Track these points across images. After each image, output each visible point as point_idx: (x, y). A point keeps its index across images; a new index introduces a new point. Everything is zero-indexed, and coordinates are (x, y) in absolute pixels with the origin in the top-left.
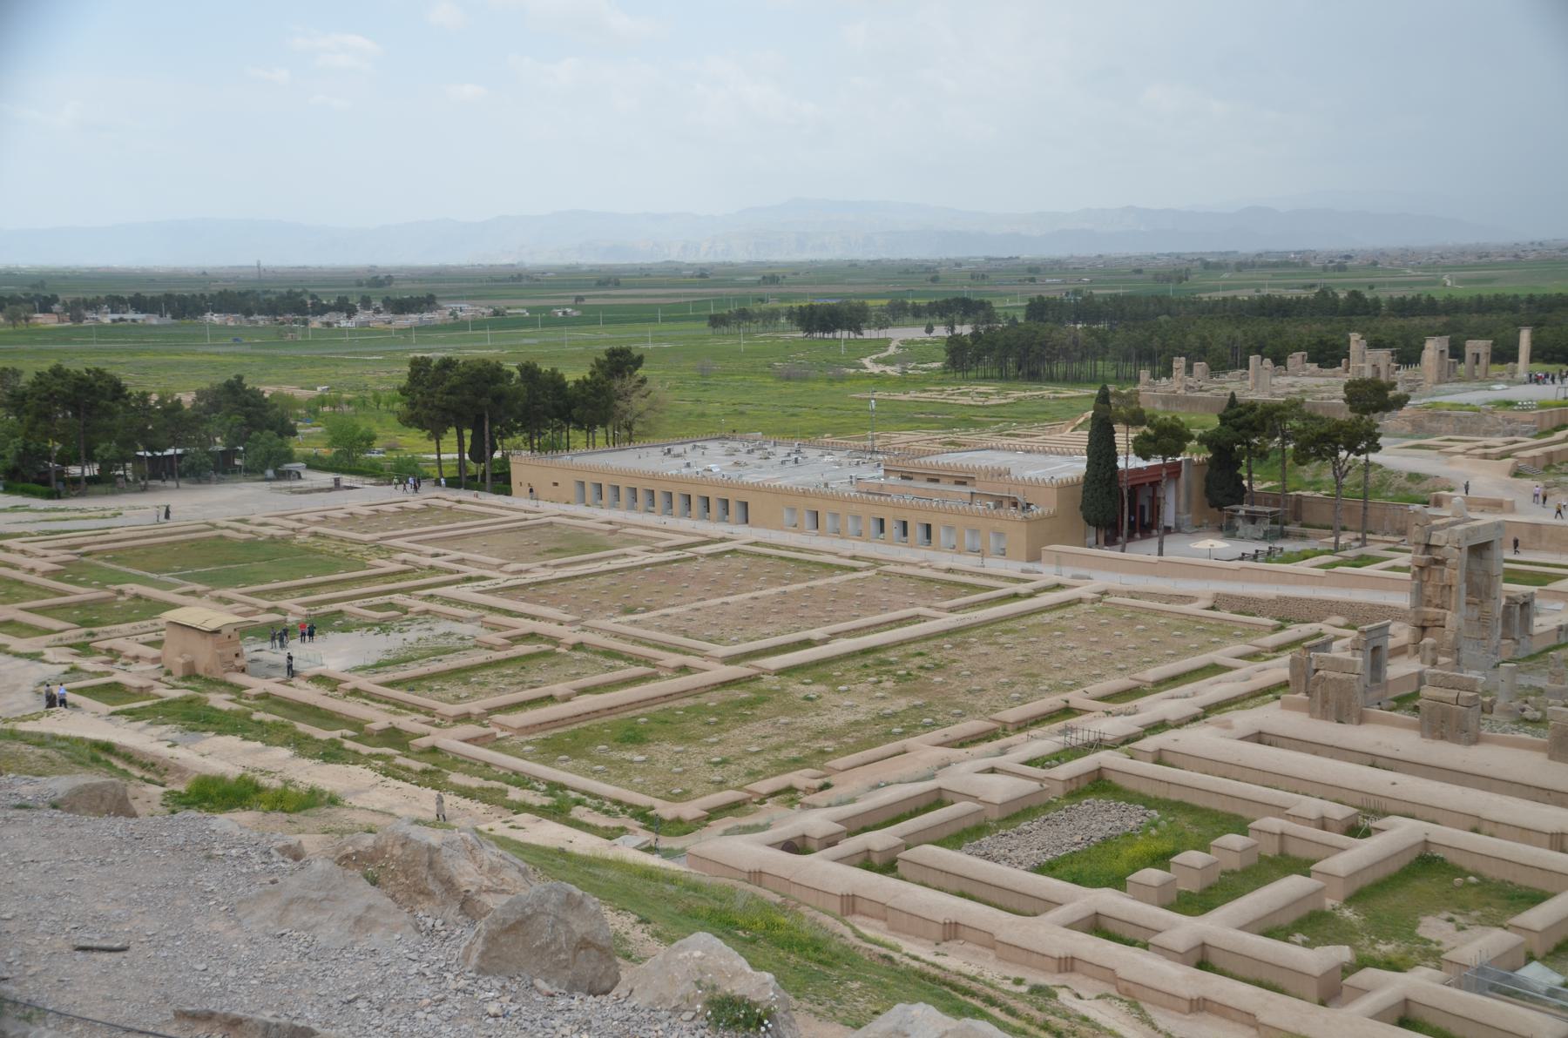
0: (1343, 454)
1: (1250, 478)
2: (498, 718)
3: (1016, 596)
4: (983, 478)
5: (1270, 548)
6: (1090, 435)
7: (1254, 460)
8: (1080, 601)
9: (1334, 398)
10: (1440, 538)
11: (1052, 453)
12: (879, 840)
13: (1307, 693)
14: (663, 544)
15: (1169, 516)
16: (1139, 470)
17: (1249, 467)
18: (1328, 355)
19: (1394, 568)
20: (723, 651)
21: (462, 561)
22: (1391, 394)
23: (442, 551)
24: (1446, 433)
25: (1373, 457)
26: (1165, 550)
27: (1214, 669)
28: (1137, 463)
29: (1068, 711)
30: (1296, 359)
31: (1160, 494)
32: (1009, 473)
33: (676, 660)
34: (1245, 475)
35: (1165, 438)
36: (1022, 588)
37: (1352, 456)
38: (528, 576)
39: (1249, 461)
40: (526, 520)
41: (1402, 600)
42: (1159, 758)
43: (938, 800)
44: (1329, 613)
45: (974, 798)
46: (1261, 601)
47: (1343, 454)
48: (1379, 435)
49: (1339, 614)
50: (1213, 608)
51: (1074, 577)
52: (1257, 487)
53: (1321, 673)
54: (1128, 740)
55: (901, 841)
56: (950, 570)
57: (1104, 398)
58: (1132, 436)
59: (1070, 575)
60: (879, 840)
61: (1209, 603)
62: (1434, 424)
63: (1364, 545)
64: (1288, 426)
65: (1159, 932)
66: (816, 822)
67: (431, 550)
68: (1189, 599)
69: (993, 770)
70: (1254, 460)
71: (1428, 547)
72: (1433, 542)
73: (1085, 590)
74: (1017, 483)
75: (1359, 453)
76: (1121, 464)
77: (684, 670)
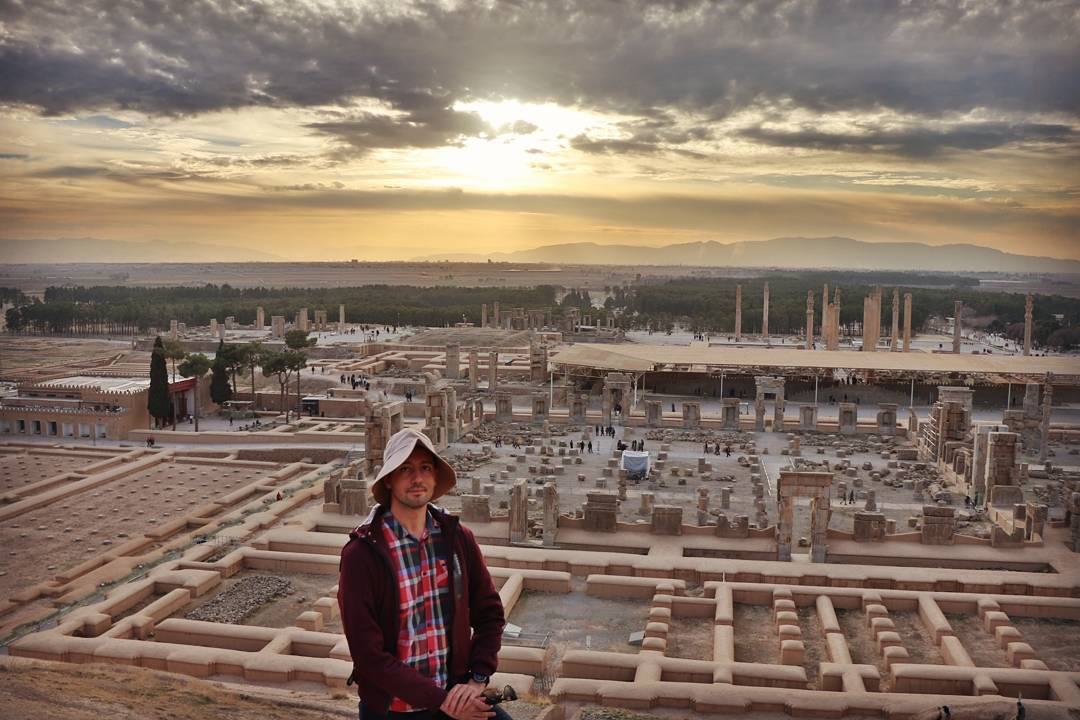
1: (235, 385)
3: (124, 461)
6: (151, 366)
7: (236, 376)
8: (163, 461)
10: (378, 413)
12: (140, 618)
13: (338, 502)
15: (191, 407)
17: (234, 379)
18: (246, 319)
19: (320, 430)
22: (308, 338)
24: (320, 358)
25: (301, 371)
26: (200, 427)
27: (257, 493)
28: (179, 379)
30: (229, 320)
31: (186, 396)
34: (232, 384)
35: (192, 368)
37: (293, 372)
41: (361, 448)
43: (158, 590)
47: (288, 371)
49: (308, 456)
52: (239, 389)
55: (106, 616)
60: (140, 618)
62: (315, 354)
63: (299, 419)
65: (334, 646)
68: (226, 455)
69: (181, 567)
70: (236, 376)
71: (372, 418)
72: (375, 415)
76: (170, 381)
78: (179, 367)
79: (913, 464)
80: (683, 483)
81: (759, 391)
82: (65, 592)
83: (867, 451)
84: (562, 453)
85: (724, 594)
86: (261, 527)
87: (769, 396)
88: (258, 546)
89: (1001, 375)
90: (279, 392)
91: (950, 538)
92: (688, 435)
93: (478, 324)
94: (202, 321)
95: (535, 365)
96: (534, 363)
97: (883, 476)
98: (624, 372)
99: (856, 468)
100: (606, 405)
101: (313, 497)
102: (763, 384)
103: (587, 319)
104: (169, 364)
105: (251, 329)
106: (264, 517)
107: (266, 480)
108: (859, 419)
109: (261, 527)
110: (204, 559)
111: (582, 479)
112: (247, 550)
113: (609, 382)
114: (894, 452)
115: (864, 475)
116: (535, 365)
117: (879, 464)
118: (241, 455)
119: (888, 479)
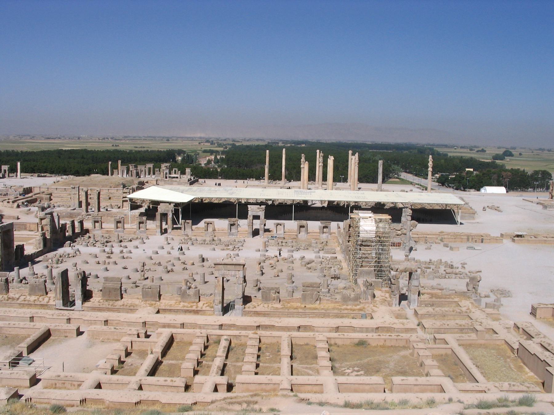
79: (330, 256)
80: (184, 269)
81: (249, 214)
83: (307, 249)
84: (122, 252)
85: (166, 334)
87: (256, 217)
89: (402, 203)
91: (317, 300)
92: (205, 241)
93: (105, 172)
95: (124, 199)
96: (124, 198)
97: (308, 264)
98: (170, 203)
99: (295, 259)
100: (158, 222)
102: (253, 210)
103: (175, 171)
108: (309, 230)
111: (125, 268)
113: (161, 209)
114: (323, 250)
115: (297, 264)
116: (124, 199)
117: (310, 255)
119: (309, 266)
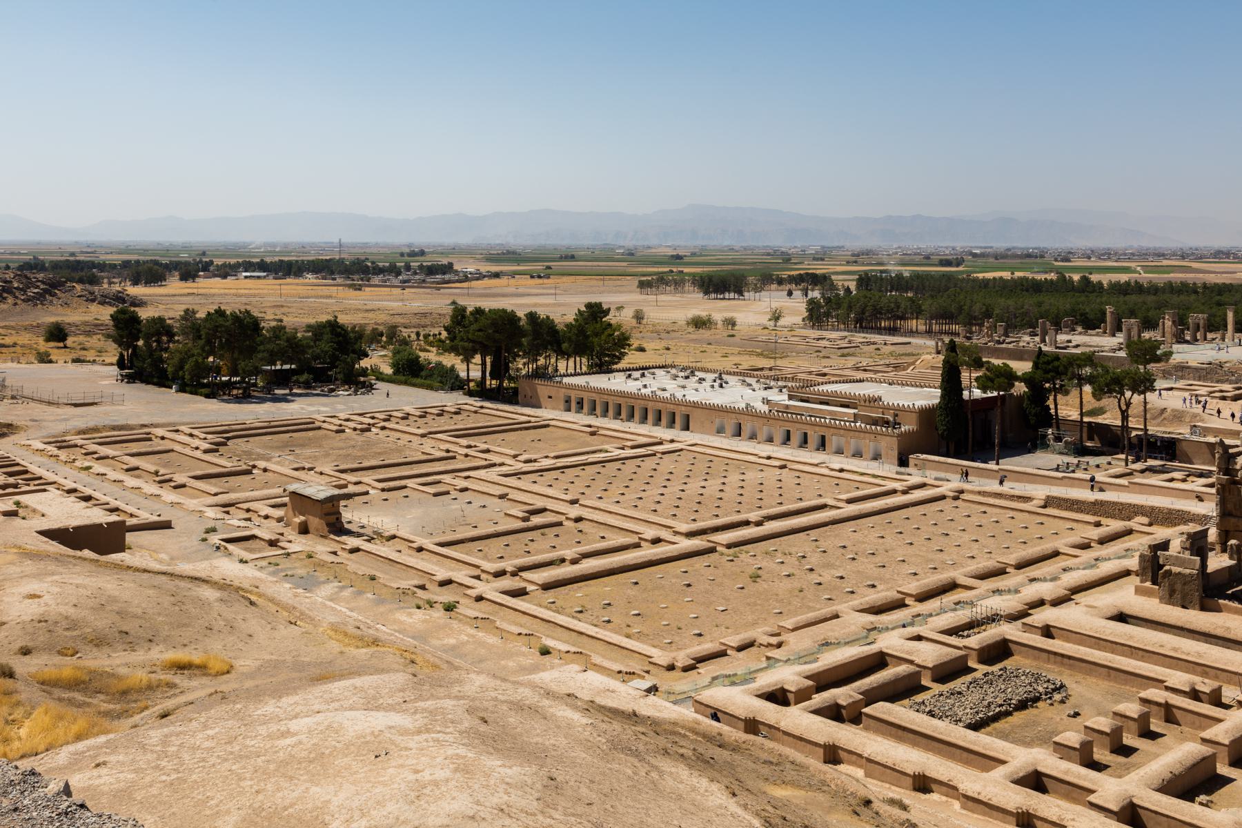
0: (1128, 394)
2: (525, 575)
3: (894, 492)
4: (862, 403)
5: (1079, 461)
8: (943, 497)
9: (1102, 352)
11: (908, 385)
14: (629, 444)
16: (976, 401)
17: (1055, 400)
18: (1091, 323)
20: (684, 528)
21: (488, 451)
23: (473, 444)
25: (1148, 394)
27: (1056, 554)
28: (978, 393)
29: (952, 586)
32: (881, 400)
33: (650, 533)
36: (898, 486)
38: (536, 464)
39: (1055, 396)
40: (530, 422)
42: (1048, 632)
43: (880, 661)
44: (1136, 514)
45: (911, 662)
46: (1083, 502)
47: (1128, 394)
48: (1155, 380)
49: (1143, 515)
50: (1044, 507)
51: (936, 479)
53: (1167, 568)
54: (1022, 615)
56: (841, 470)
57: (952, 347)
58: (974, 375)
59: (933, 477)
61: (1042, 503)
64: (1083, 372)
66: (790, 676)
67: (464, 442)
69: (919, 638)
70: (1059, 396)
73: (946, 488)
74: (887, 408)
75: (1140, 393)
76: (966, 394)
77: (656, 541)
78: (977, 379)
82: (779, 645)
86: (1040, 603)
88: (1029, 628)
90: (1119, 423)
94: (1028, 324)
101: (1127, 573)
104: (965, 375)
105: (1097, 335)
106: (1046, 590)
107: (1076, 538)
109: (1040, 603)
110: (954, 631)
112: (1010, 631)
118: (1049, 502)
